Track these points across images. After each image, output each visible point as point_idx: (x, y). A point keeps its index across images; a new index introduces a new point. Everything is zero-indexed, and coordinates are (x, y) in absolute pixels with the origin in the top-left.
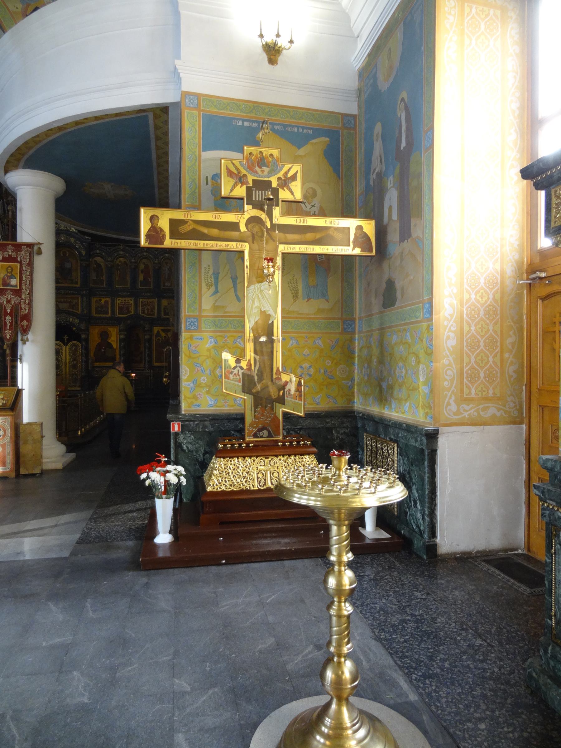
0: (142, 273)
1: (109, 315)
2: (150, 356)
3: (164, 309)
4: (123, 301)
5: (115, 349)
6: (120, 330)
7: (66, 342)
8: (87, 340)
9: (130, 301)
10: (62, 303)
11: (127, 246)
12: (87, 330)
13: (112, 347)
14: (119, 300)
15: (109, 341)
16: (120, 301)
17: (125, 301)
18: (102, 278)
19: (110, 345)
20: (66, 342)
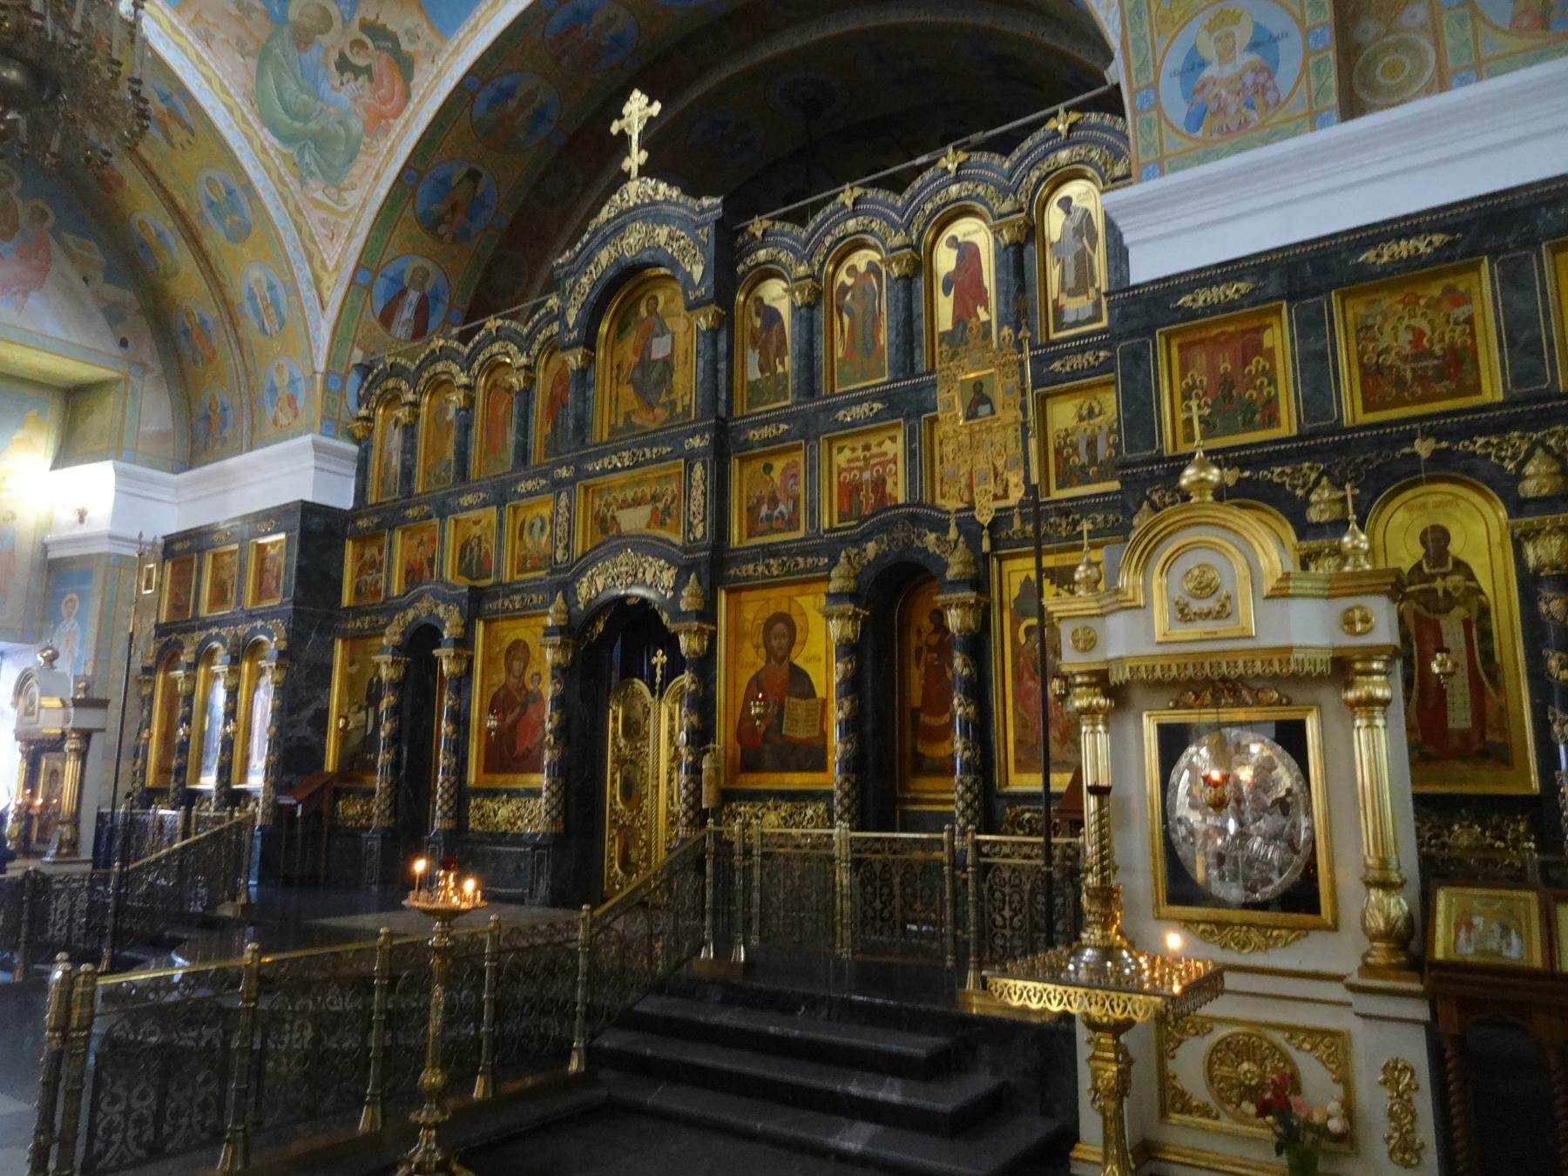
0: (946, 292)
1: (800, 534)
2: (981, 731)
3: (1058, 452)
4: (860, 453)
5: (824, 702)
6: (834, 597)
7: (658, 679)
8: (704, 665)
9: (888, 445)
10: (629, 506)
11: (873, 184)
12: (707, 614)
13: (809, 692)
14: (841, 450)
15: (799, 662)
16: (847, 453)
17: (867, 448)
18: (780, 369)
19: (799, 681)
20: (658, 679)
